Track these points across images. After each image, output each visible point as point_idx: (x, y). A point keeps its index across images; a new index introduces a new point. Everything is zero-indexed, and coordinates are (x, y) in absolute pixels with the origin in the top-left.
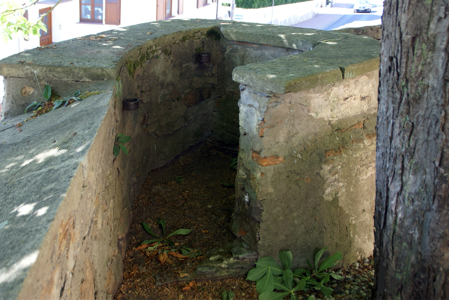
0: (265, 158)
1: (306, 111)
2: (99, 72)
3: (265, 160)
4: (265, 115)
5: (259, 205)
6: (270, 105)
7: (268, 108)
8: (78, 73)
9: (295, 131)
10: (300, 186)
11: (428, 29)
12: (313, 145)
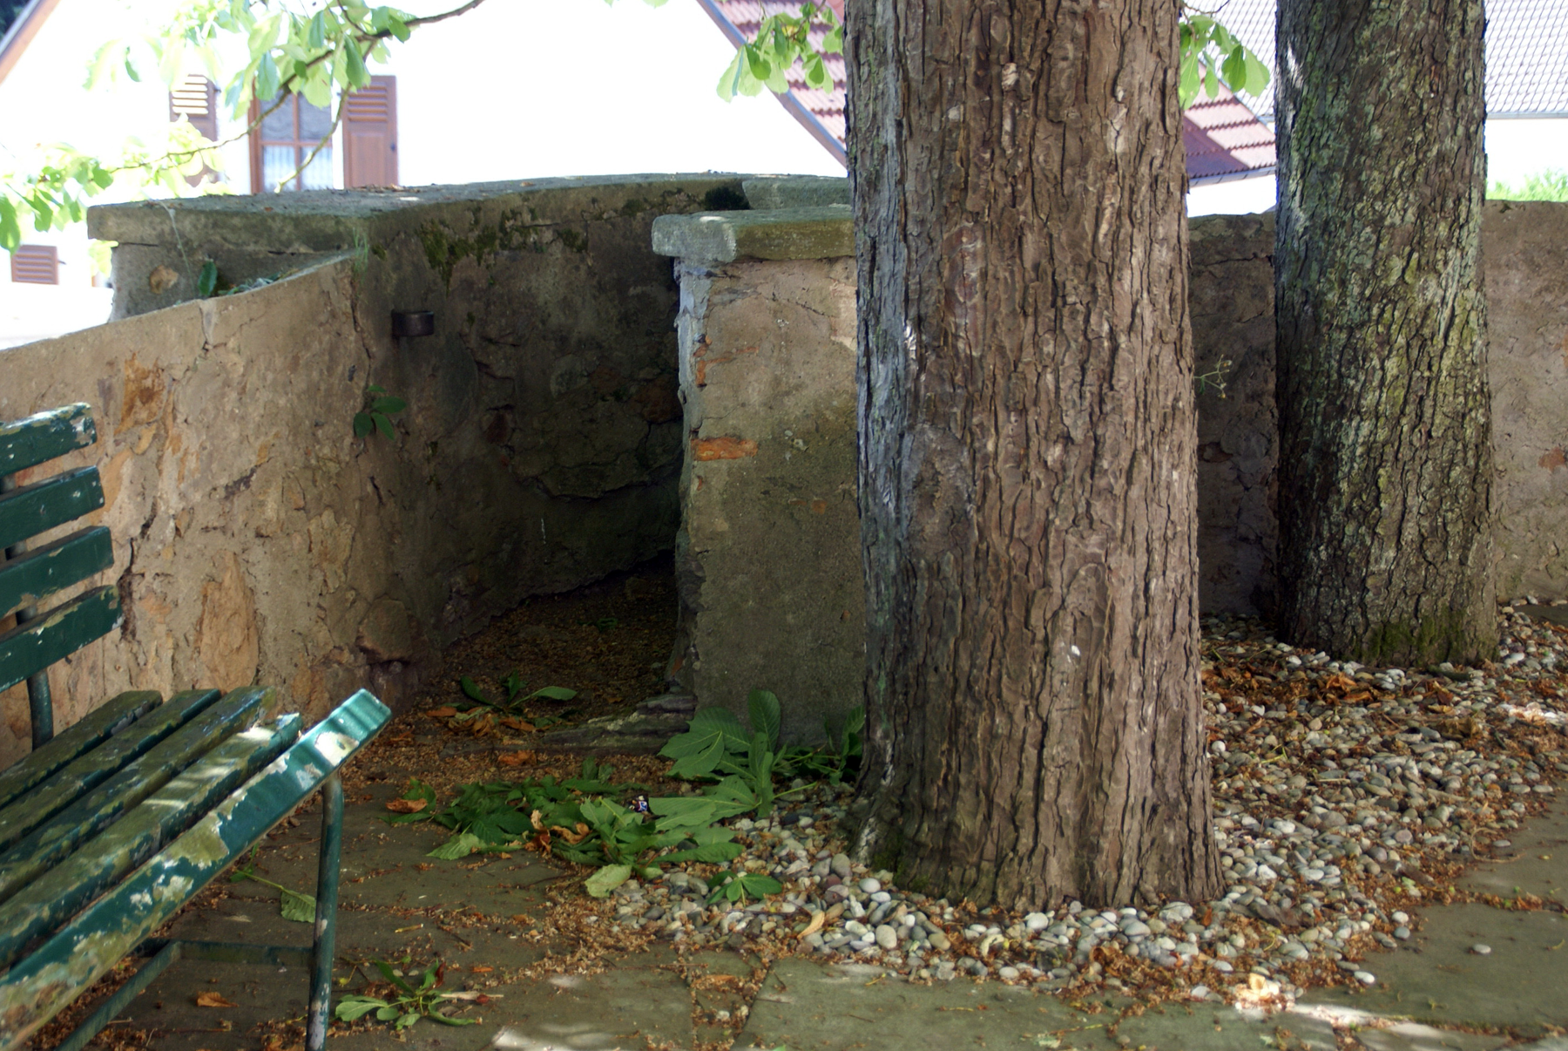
0: (708, 440)
1: (824, 329)
2: (330, 227)
3: (707, 445)
4: (705, 326)
5: (694, 565)
6: (717, 299)
7: (711, 306)
8: (281, 231)
9: (793, 382)
10: (798, 522)
11: (874, 15)
12: (841, 420)
